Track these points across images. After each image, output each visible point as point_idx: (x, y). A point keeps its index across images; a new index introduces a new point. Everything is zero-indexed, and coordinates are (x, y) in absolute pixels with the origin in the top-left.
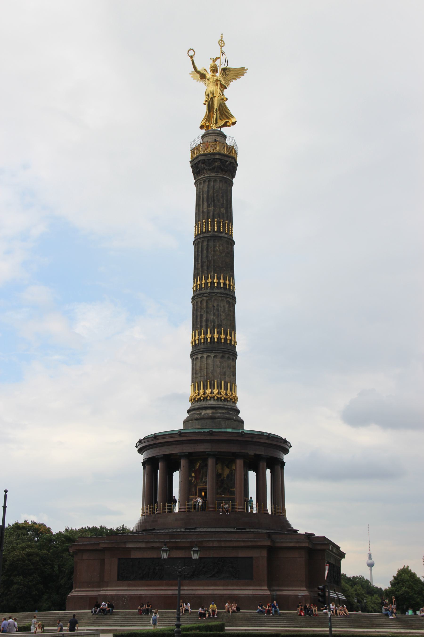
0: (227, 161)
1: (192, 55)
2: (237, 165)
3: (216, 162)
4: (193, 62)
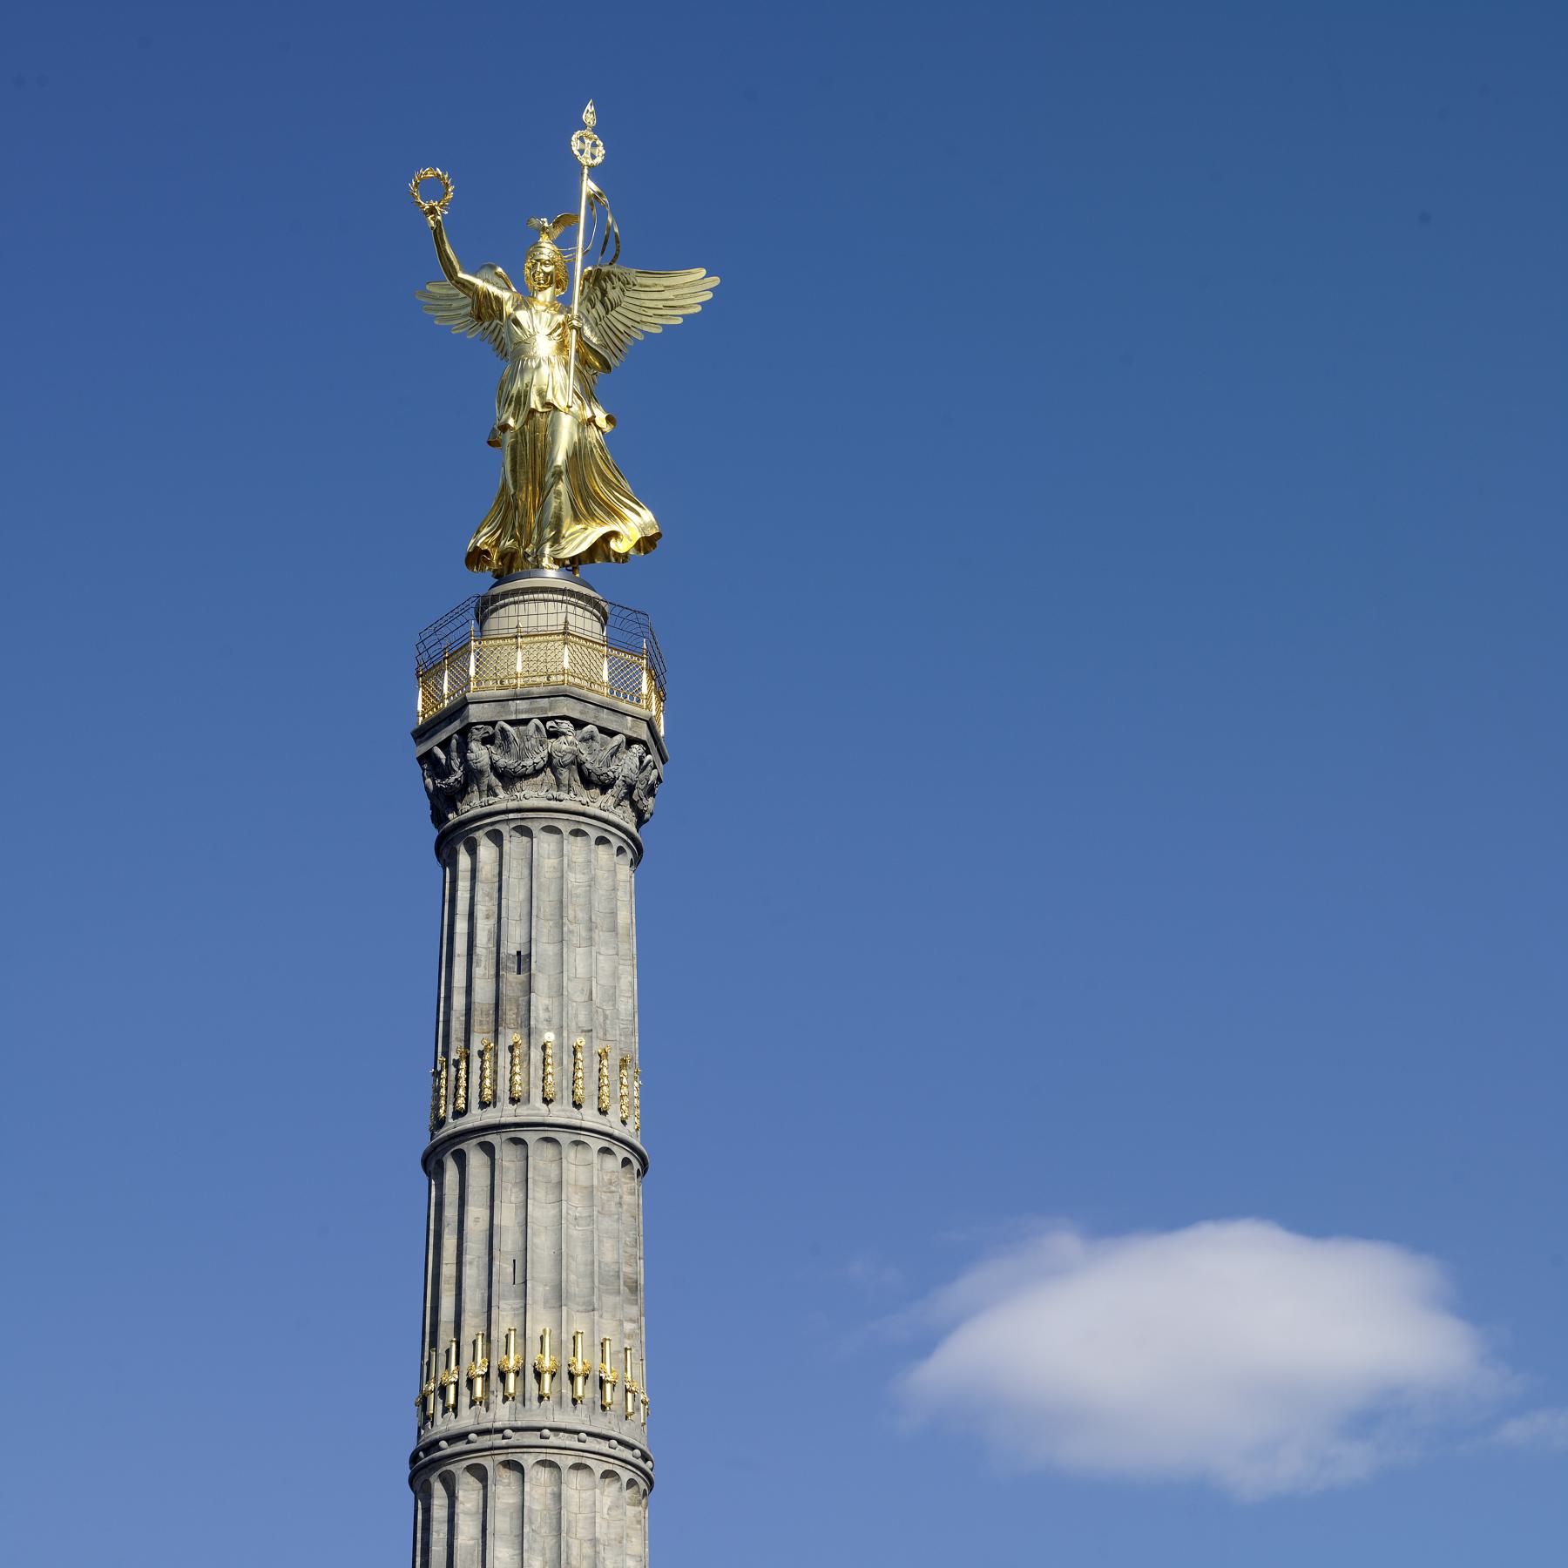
3: (553, 734)
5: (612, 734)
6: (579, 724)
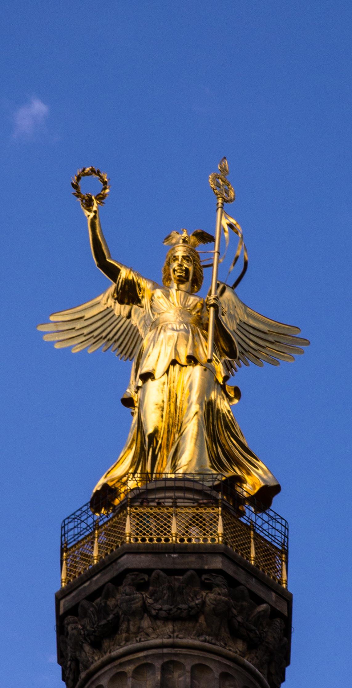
0: (264, 602)
2: (283, 680)
3: (209, 587)
5: (260, 601)
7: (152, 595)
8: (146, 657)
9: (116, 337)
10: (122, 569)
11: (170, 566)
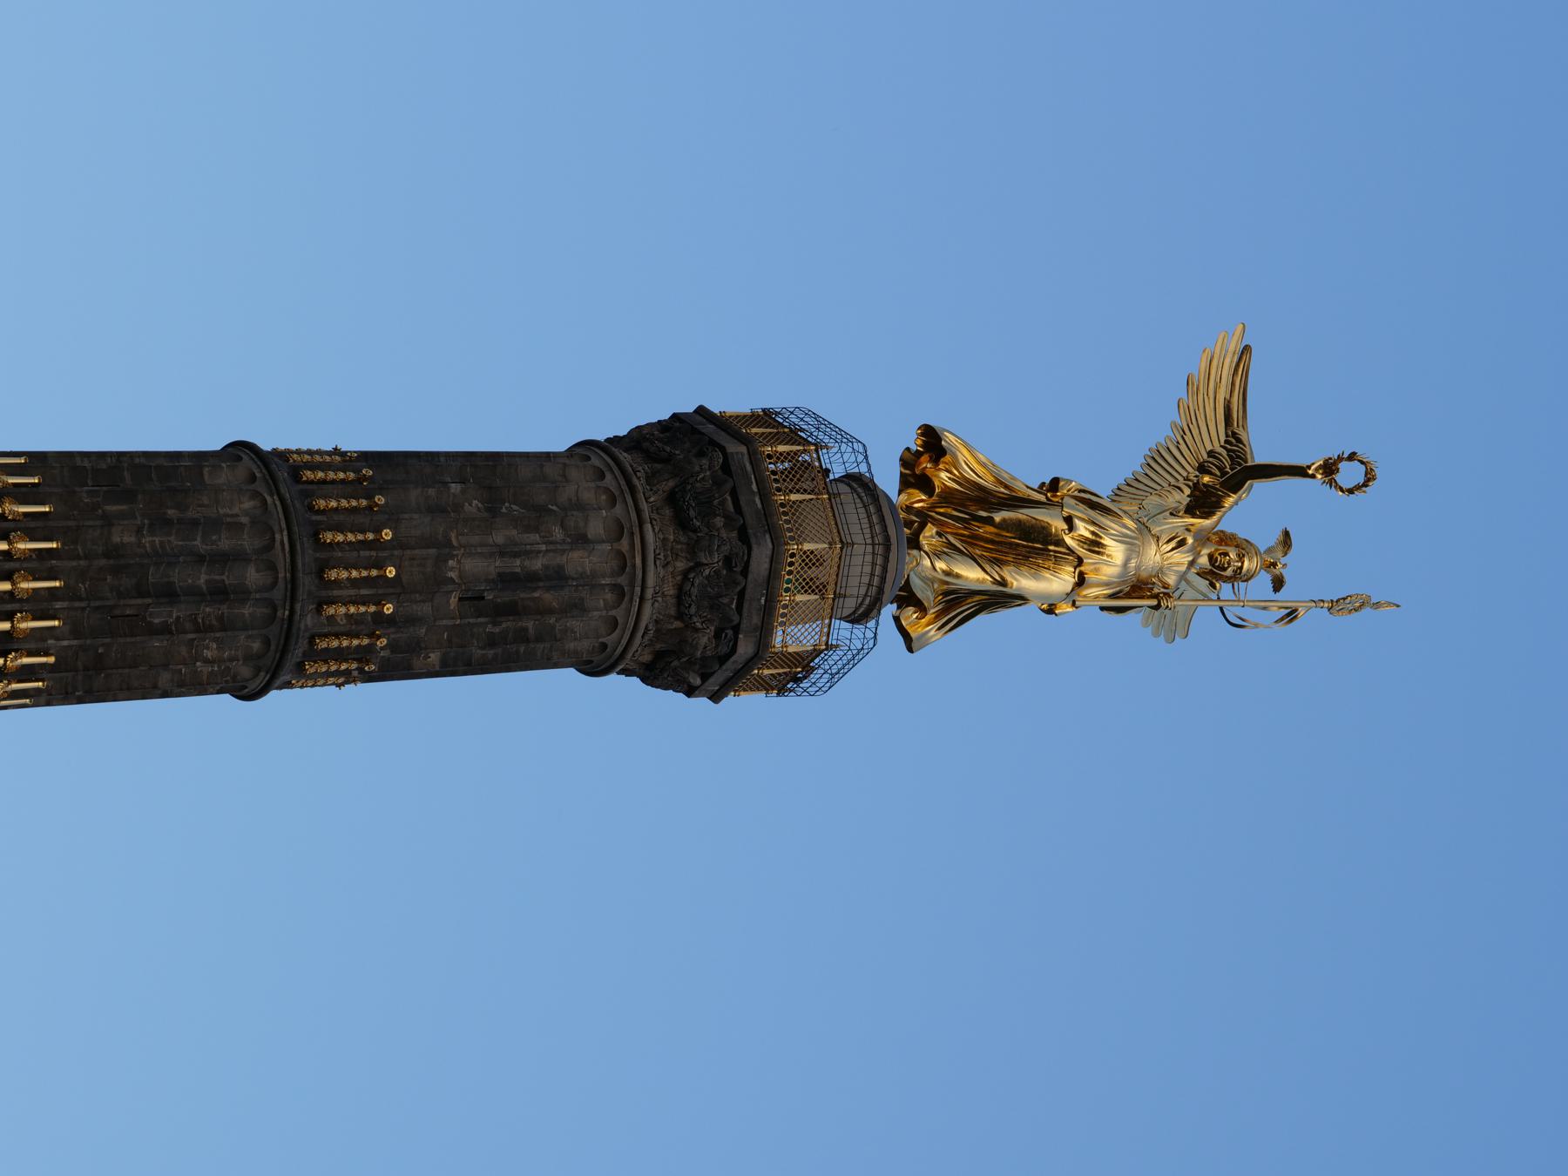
1: (1338, 477)
3: (718, 635)
4: (1299, 471)
6: (723, 660)
7: (717, 573)
8: (634, 566)
9: (1183, 447)
10: (753, 540)
11: (747, 597)
